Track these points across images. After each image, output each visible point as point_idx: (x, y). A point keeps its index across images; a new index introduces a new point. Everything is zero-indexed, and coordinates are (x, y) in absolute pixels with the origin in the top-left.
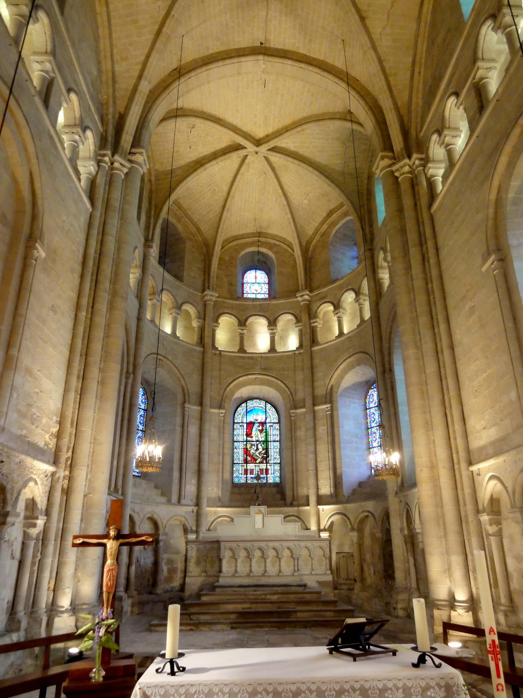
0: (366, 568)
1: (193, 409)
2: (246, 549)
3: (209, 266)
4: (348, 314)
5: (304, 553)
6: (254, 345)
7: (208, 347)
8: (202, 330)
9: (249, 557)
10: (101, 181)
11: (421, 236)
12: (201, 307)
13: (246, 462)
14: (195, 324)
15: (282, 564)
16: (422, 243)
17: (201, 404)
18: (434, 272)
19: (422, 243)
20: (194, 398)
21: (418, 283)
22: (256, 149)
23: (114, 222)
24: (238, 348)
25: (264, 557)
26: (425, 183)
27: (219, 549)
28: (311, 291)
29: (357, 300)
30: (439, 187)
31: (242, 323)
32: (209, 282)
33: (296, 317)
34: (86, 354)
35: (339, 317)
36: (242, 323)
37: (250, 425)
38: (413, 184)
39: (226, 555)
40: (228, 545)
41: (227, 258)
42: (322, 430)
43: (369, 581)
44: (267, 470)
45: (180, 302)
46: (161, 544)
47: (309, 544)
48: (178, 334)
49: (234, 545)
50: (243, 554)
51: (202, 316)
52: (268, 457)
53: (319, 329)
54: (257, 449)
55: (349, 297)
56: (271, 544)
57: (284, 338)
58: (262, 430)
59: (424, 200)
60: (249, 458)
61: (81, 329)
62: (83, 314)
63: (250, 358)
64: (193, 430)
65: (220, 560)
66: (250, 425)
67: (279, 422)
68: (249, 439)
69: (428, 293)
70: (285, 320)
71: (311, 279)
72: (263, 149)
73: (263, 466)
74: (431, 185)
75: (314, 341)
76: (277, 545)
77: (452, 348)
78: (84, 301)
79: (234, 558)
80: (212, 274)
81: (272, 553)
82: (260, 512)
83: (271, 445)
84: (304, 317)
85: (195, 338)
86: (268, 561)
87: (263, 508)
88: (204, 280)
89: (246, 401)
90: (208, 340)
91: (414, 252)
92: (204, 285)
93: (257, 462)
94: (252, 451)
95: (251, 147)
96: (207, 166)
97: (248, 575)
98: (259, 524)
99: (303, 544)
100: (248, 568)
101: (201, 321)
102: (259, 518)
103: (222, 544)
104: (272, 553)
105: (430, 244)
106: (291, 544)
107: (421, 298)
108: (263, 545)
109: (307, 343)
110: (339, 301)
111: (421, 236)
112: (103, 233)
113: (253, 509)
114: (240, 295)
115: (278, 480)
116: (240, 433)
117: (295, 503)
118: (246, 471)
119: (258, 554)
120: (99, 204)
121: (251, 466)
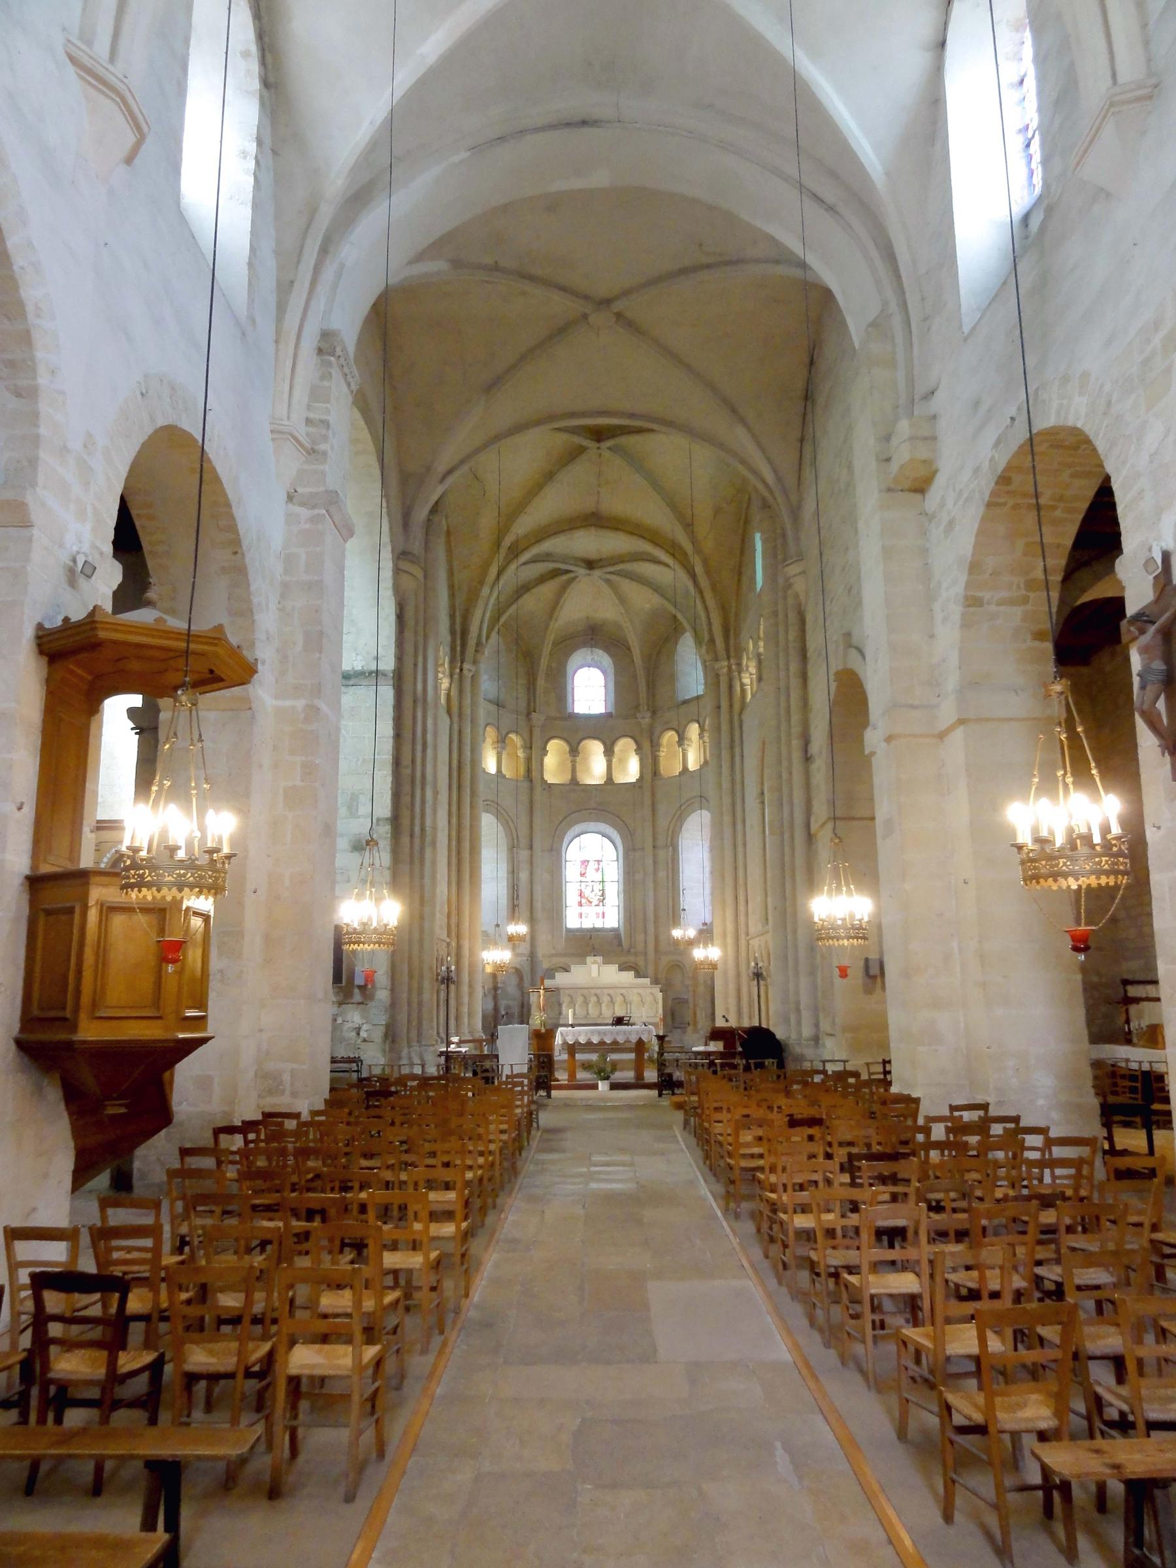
0: (698, 1012)
1: (524, 854)
2: (583, 995)
3: (535, 680)
4: (694, 745)
5: (636, 999)
6: (588, 770)
7: (537, 782)
8: (529, 760)
9: (586, 1002)
10: (454, 693)
11: (732, 741)
12: (526, 735)
13: (580, 904)
14: (521, 754)
15: (616, 1009)
16: (732, 747)
17: (531, 848)
18: (738, 777)
19: (732, 747)
20: (524, 841)
21: (726, 785)
22: (588, 572)
23: (467, 731)
24: (570, 777)
25: (599, 1003)
26: (738, 689)
27: (559, 994)
28: (654, 713)
29: (701, 736)
30: (749, 696)
31: (574, 751)
32: (535, 701)
33: (636, 741)
34: (459, 853)
35: (683, 750)
36: (574, 751)
37: (585, 863)
38: (731, 687)
39: (565, 1000)
40: (566, 991)
41: (554, 665)
42: (662, 874)
43: (700, 1026)
44: (603, 914)
45: (504, 733)
46: (499, 991)
47: (641, 991)
48: (504, 771)
49: (571, 992)
50: (580, 1000)
51: (528, 745)
52: (604, 899)
53: (661, 759)
54: (593, 891)
55: (693, 730)
56: (606, 991)
57: (623, 761)
58: (597, 870)
59: (737, 706)
60: (584, 901)
61: (454, 833)
62: (454, 820)
63: (583, 791)
64: (524, 876)
65: (560, 1005)
66: (585, 863)
67: (617, 860)
68: (583, 879)
69: (733, 793)
70: (625, 745)
71: (654, 696)
72: (597, 573)
73: (600, 909)
74: (743, 691)
75: (656, 773)
76: (611, 992)
77: (745, 845)
78: (454, 808)
79: (572, 1004)
80: (538, 692)
81: (606, 999)
82: (595, 962)
83: (608, 886)
84: (646, 745)
85: (522, 770)
86: (603, 1005)
87: (599, 959)
88: (529, 700)
89: (579, 835)
90: (535, 774)
91: (725, 754)
92: (529, 704)
93: (593, 904)
94: (587, 892)
95: (581, 571)
96: (534, 590)
97: (585, 1017)
98: (594, 973)
99: (635, 991)
100: (585, 1012)
101: (528, 751)
102: (595, 967)
103: (561, 991)
104: (606, 999)
105: (737, 751)
106: (623, 991)
107: (727, 800)
108: (598, 991)
109: (648, 777)
110: (684, 731)
111: (732, 741)
112: (460, 742)
113: (589, 959)
114: (570, 711)
115: (616, 925)
116: (571, 872)
117: (633, 950)
118: (581, 915)
119: (593, 999)
120: (456, 719)
121: (585, 909)
